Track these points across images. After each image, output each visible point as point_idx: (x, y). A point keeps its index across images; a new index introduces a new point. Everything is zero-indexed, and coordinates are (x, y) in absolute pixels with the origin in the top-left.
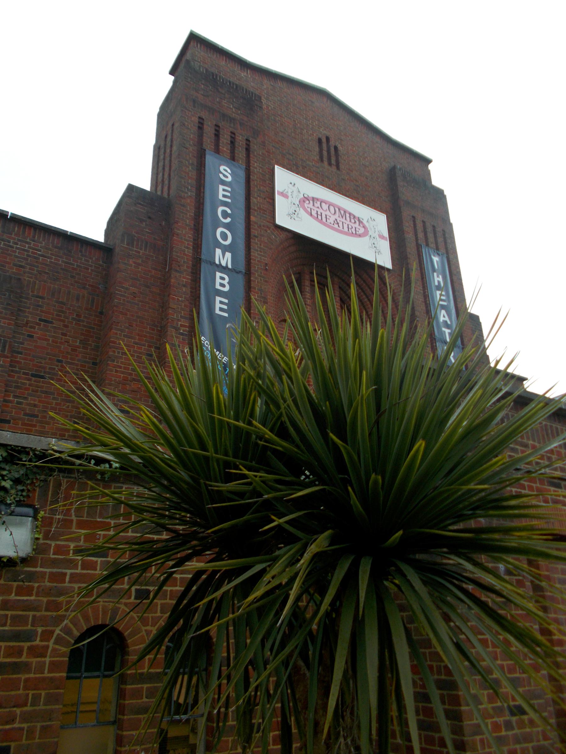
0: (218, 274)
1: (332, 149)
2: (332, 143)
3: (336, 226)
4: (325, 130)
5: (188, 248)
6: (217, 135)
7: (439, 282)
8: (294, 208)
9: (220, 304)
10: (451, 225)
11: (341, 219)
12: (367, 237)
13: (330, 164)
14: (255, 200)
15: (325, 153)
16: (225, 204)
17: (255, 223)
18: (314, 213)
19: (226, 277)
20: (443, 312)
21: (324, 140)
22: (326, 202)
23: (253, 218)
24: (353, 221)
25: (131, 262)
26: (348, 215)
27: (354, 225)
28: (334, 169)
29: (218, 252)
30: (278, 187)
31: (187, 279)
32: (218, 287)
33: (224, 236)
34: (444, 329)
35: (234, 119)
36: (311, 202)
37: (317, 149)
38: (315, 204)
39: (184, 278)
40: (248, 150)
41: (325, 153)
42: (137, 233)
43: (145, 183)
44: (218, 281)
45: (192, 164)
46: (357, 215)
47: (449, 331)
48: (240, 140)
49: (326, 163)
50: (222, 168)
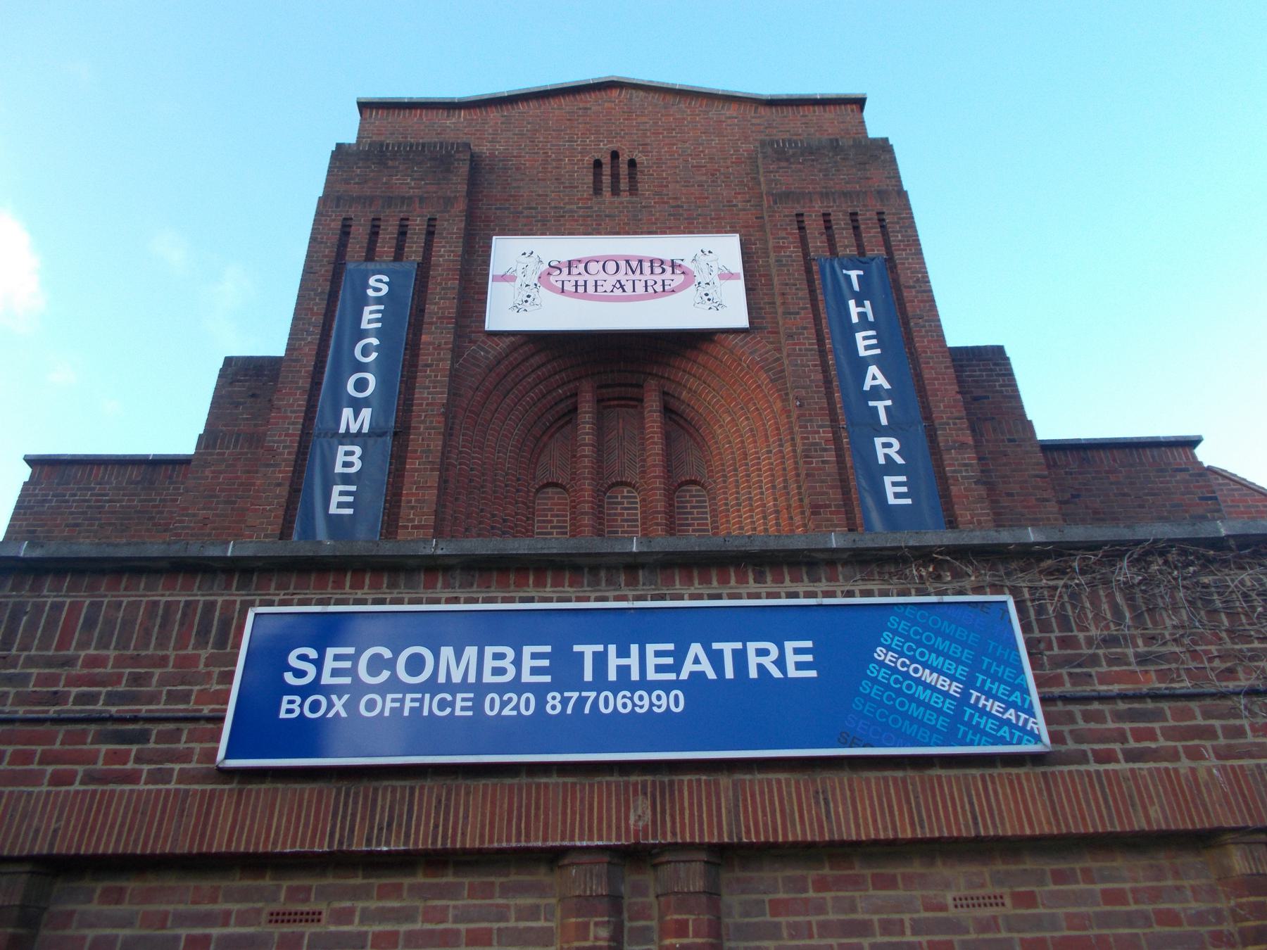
0: (342, 449)
1: (624, 169)
2: (624, 158)
3: (618, 292)
4: (610, 142)
5: (293, 423)
6: (374, 234)
7: (862, 316)
8: (527, 291)
10: (903, 195)
11: (631, 277)
12: (693, 287)
13: (615, 191)
14: (435, 308)
15: (606, 179)
17: (430, 344)
18: (569, 287)
19: (358, 450)
20: (873, 370)
21: (606, 160)
23: (424, 338)
24: (658, 270)
25: (207, 472)
26: (646, 265)
27: (659, 279)
28: (625, 198)
29: (347, 413)
30: (496, 267)
31: (286, 472)
33: (361, 385)
34: (871, 404)
35: (410, 198)
36: (565, 270)
38: (574, 271)
39: (280, 472)
40: (430, 234)
41: (606, 179)
42: (225, 425)
43: (275, 345)
45: (322, 292)
46: (667, 257)
47: (889, 403)
48: (417, 225)
49: (608, 194)
50: (372, 282)
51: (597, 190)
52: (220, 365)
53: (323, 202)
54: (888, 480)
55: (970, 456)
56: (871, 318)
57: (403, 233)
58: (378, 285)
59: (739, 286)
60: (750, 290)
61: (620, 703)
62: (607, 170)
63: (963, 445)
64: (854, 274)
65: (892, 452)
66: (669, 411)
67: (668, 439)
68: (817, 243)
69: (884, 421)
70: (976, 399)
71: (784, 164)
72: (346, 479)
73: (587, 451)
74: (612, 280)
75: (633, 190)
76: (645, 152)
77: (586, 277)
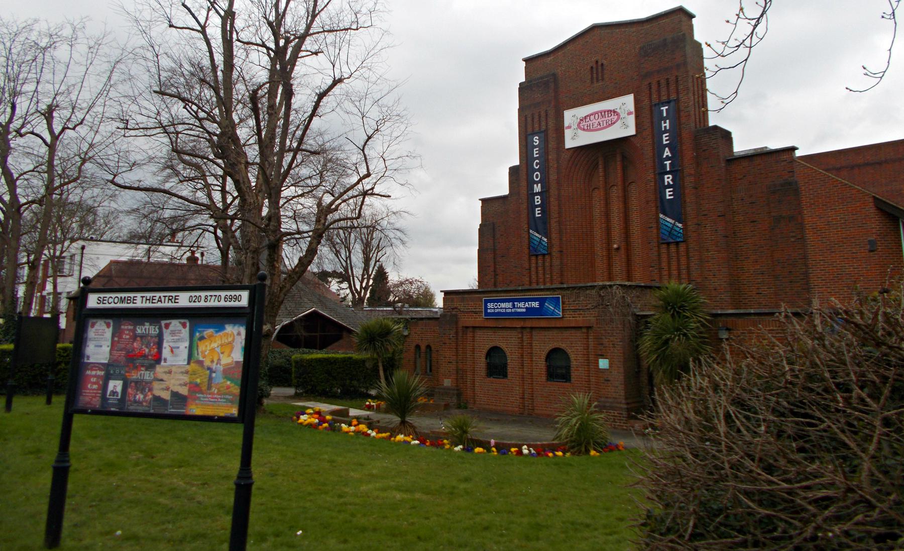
2: (600, 63)
3: (599, 127)
7: (665, 127)
9: (538, 211)
15: (595, 75)
16: (537, 158)
18: (586, 128)
20: (667, 149)
21: (595, 66)
22: (592, 114)
23: (550, 157)
27: (610, 118)
29: (535, 185)
30: (566, 124)
32: (536, 204)
33: (537, 177)
37: (590, 77)
40: (547, 115)
41: (595, 75)
44: (536, 200)
51: (592, 78)
52: (508, 171)
53: (519, 110)
54: (668, 190)
55: (692, 179)
56: (668, 128)
57: (540, 117)
58: (536, 139)
59: (632, 117)
60: (637, 117)
61: (519, 310)
62: (595, 72)
63: (691, 175)
64: (664, 109)
65: (669, 180)
66: (624, 158)
67: (624, 169)
68: (654, 96)
69: (668, 169)
70: (704, 151)
71: (647, 58)
72: (537, 206)
73: (601, 179)
74: (597, 122)
75: (603, 79)
76: (606, 59)
77: (590, 122)
